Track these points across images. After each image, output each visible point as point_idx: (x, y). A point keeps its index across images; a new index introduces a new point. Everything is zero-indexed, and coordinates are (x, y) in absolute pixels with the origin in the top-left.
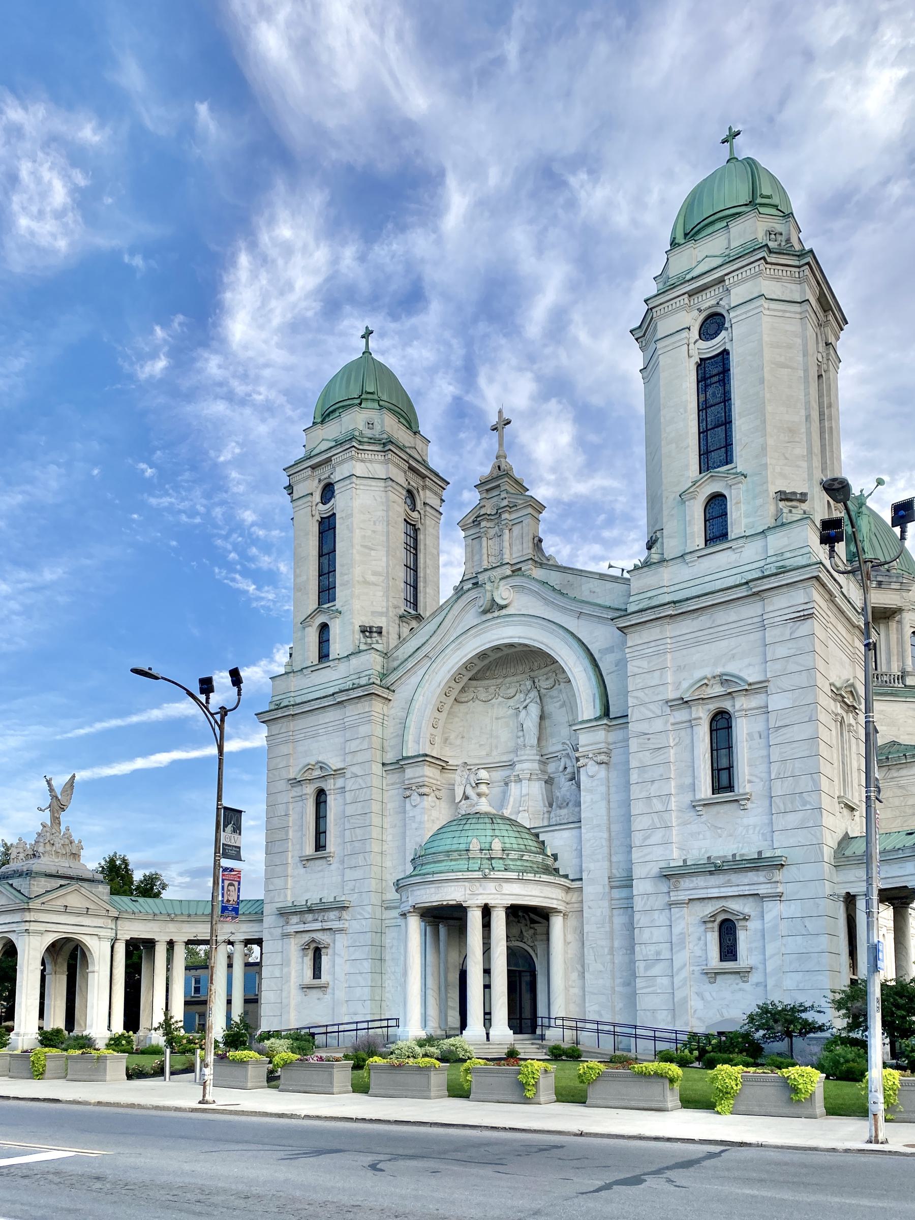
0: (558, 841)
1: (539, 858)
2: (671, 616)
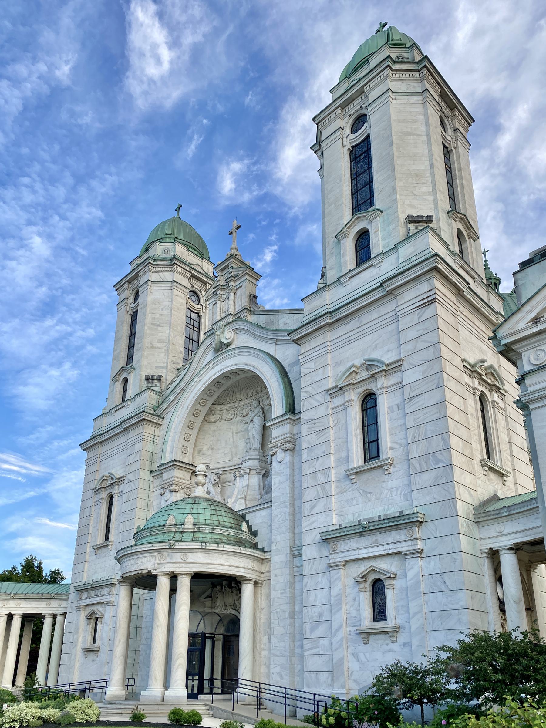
1: (232, 532)
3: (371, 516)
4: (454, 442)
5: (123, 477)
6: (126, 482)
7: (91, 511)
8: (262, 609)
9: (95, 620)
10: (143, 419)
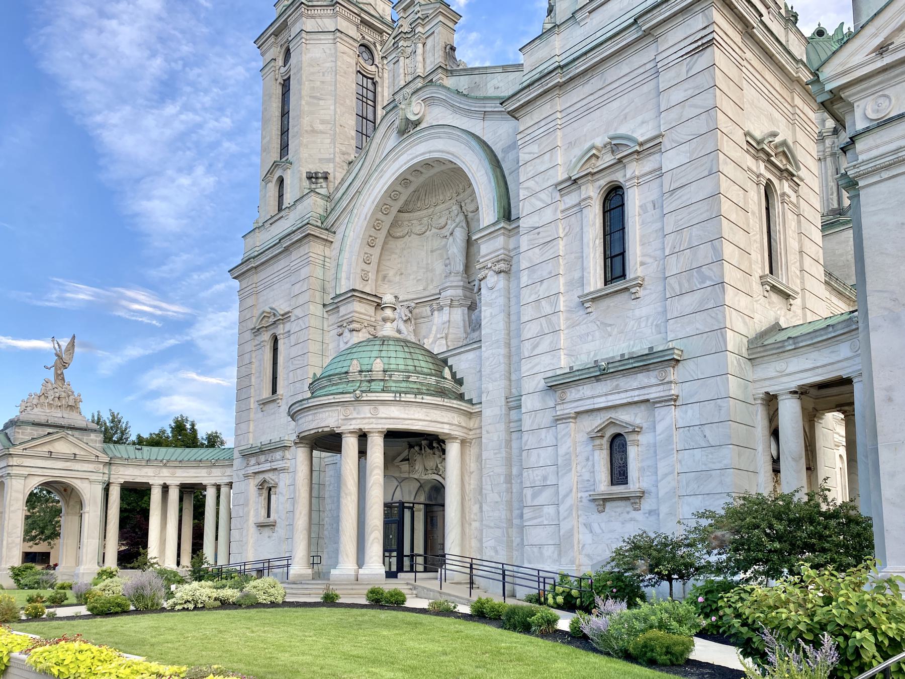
0: (462, 364)
1: (432, 380)
2: (560, 86)
3: (611, 355)
4: (729, 251)
5: (288, 312)
6: (293, 319)
7: (251, 358)
8: (471, 473)
9: (268, 490)
10: (309, 234)
